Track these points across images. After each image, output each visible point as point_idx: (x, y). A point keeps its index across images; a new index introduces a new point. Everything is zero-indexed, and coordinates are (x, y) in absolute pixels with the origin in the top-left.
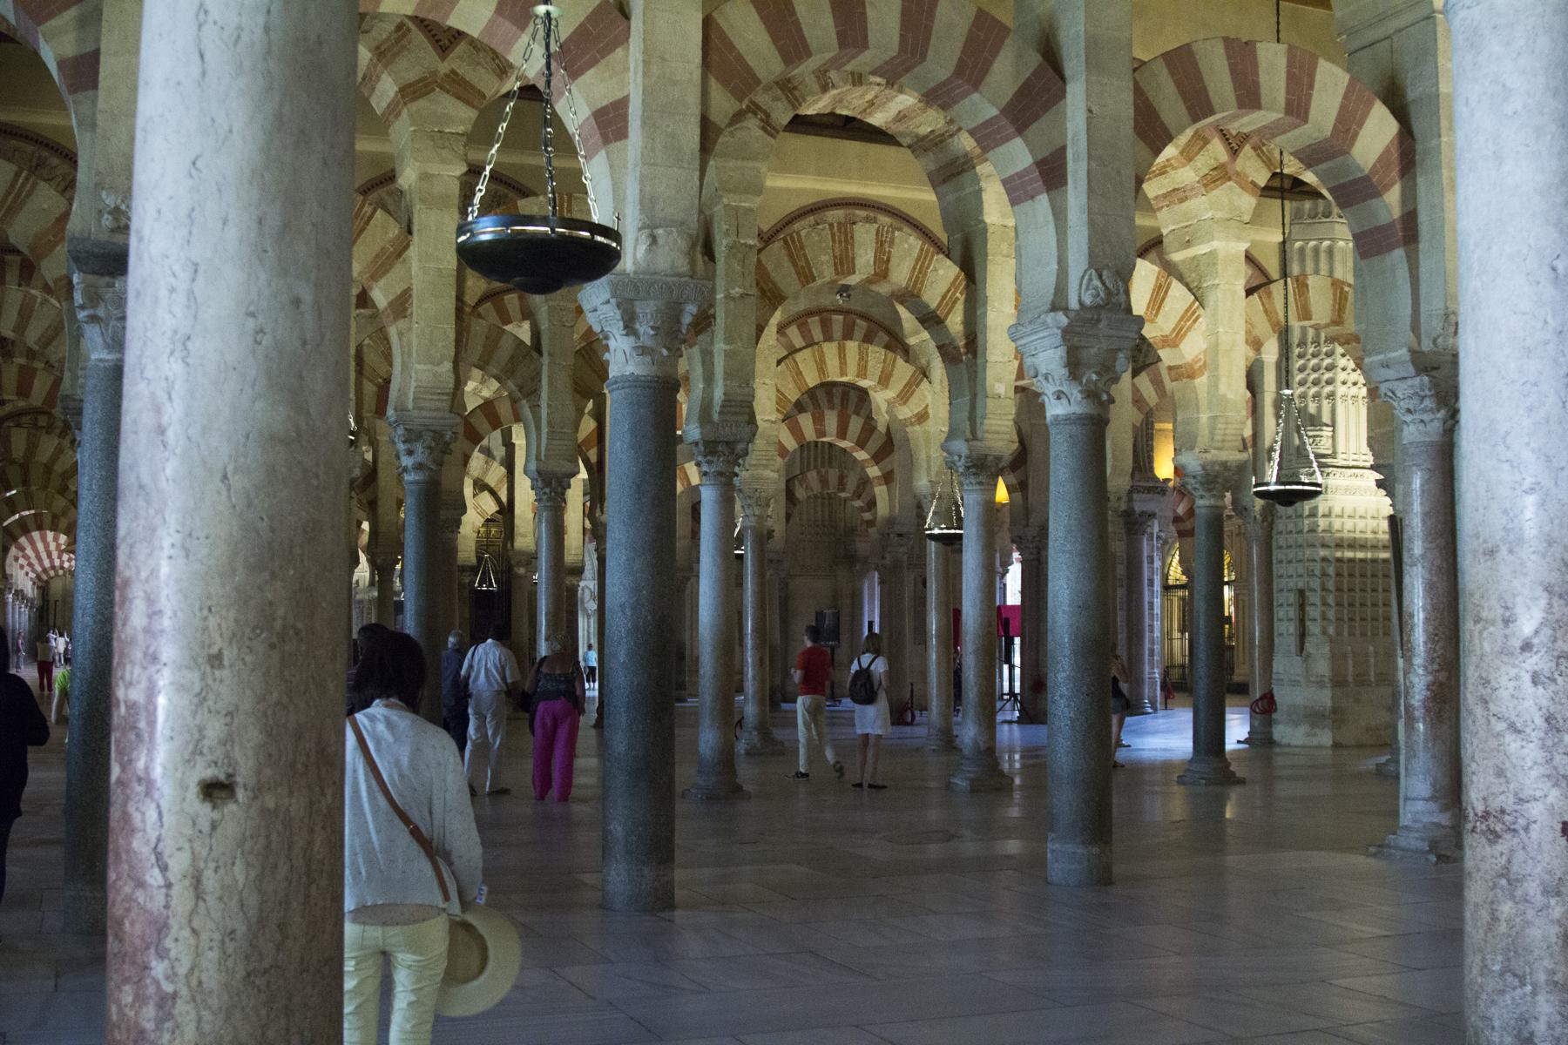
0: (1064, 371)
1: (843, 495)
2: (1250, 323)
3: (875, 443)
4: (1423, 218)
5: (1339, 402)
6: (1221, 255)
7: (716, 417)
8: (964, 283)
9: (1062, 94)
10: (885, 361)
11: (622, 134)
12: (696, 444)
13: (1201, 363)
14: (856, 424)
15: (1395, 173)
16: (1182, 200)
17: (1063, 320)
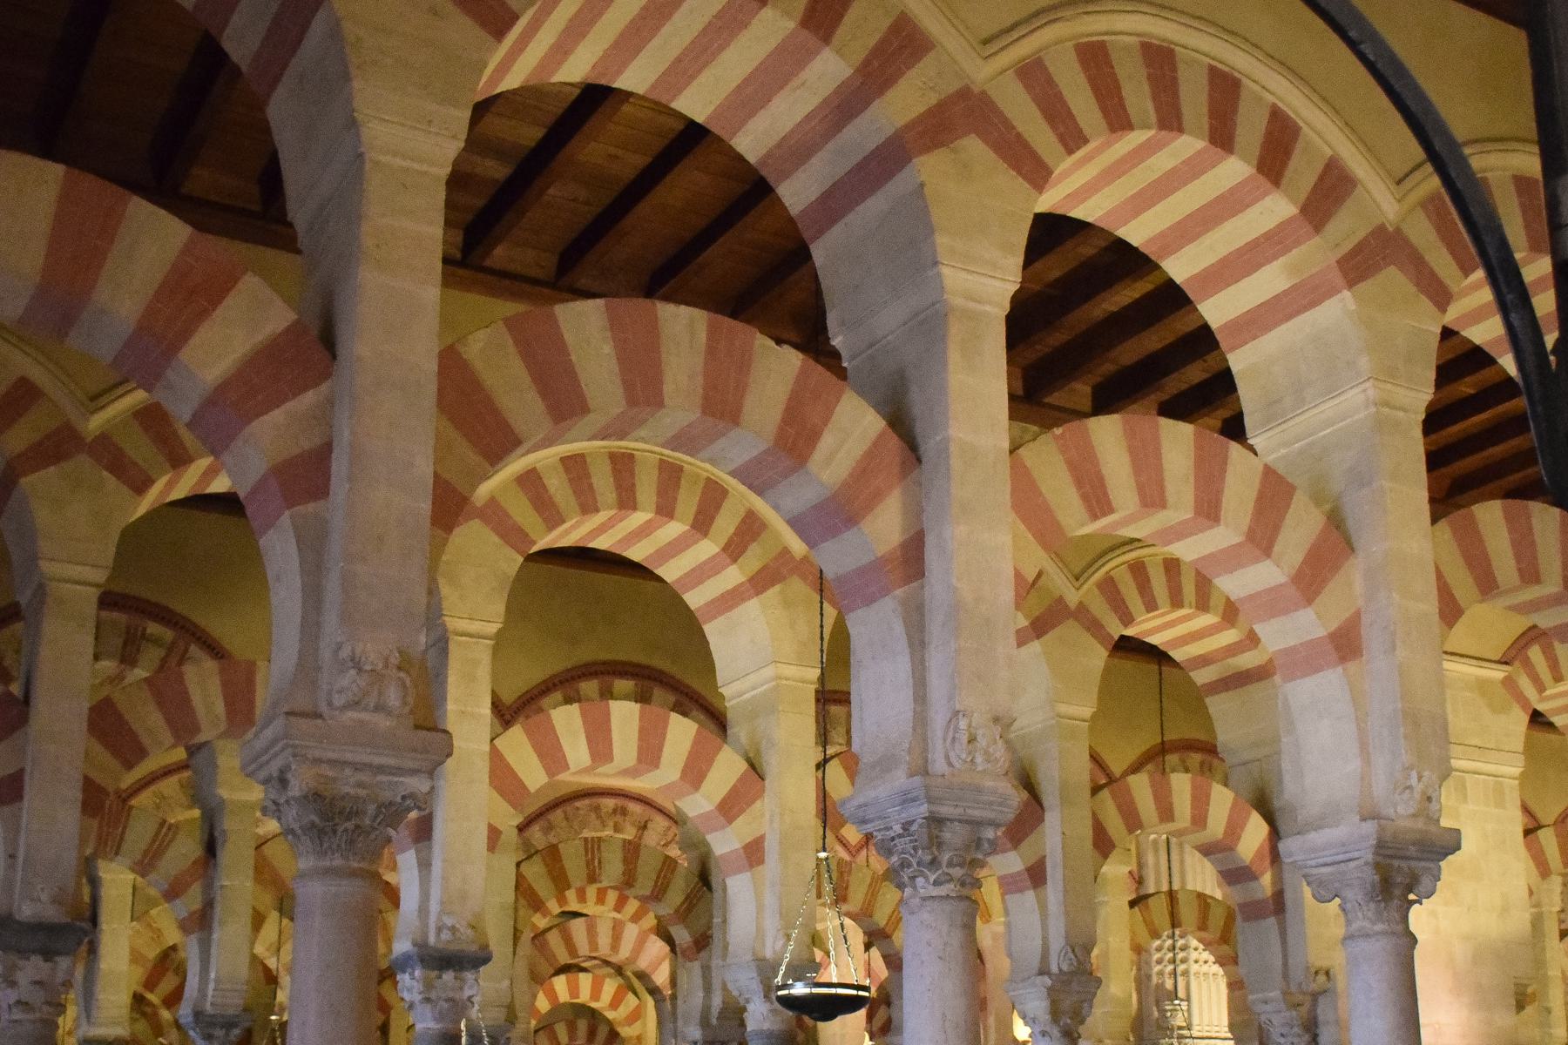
0: (1048, 1017)
2: (1133, 934)
4: (1288, 896)
5: (1192, 978)
7: (714, 1021)
9: (1041, 820)
11: (761, 861)
15: (1267, 862)
17: (1049, 982)
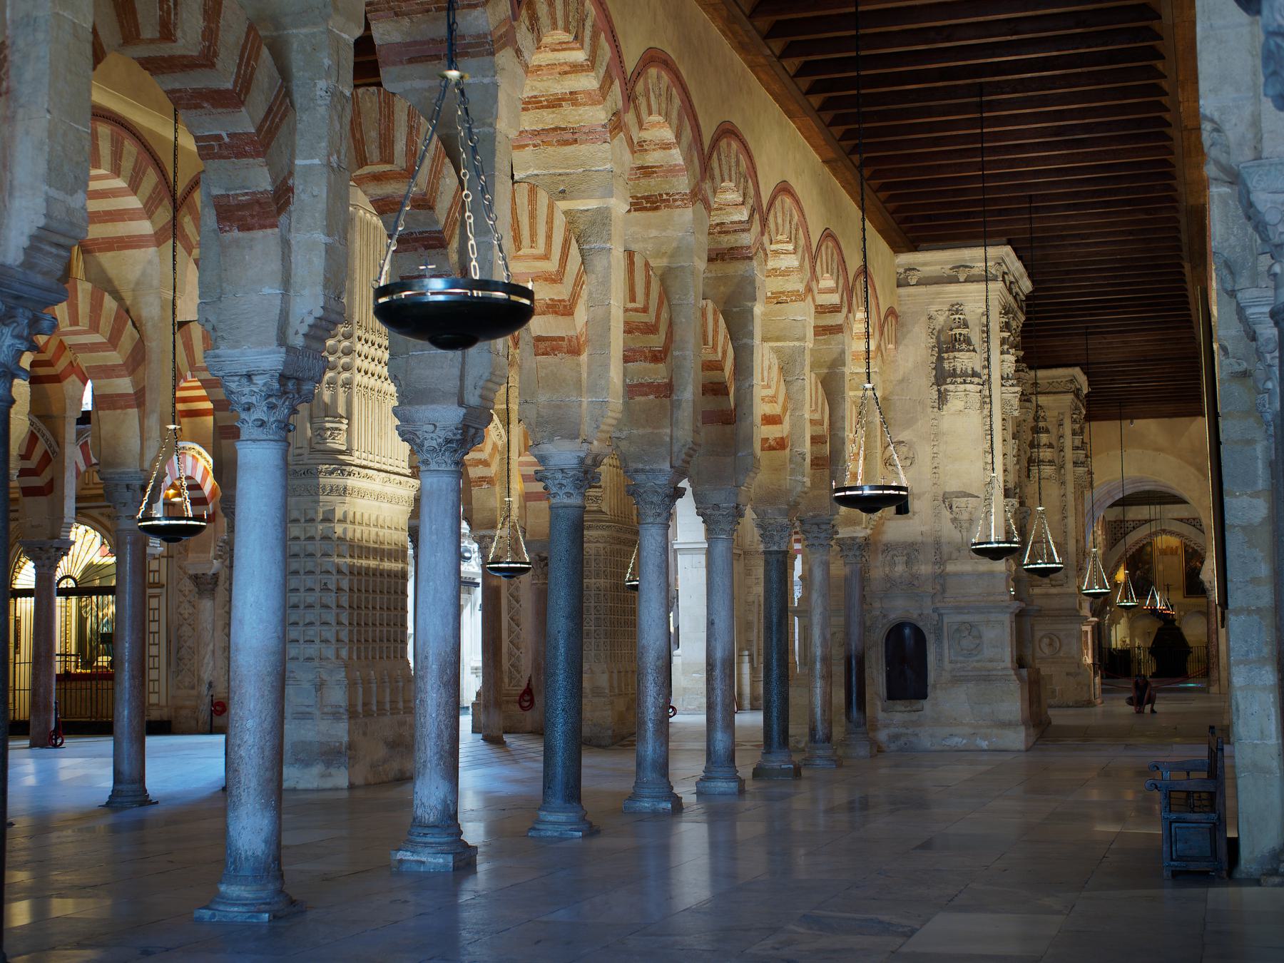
12: (249, 376)
16: (566, 143)
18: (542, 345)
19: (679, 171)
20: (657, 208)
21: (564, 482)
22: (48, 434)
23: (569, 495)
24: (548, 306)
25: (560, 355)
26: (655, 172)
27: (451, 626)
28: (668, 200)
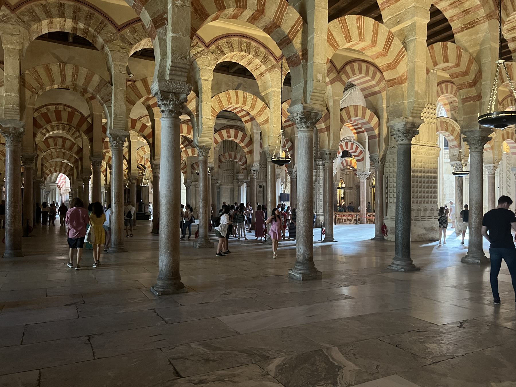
1: (236, 160)
3: (247, 140)
6: (418, 24)
8: (302, 23)
10: (253, 99)
13: (405, 77)
14: (240, 134)
18: (390, 83)
19: (479, 7)
20: (473, 26)
21: (400, 135)
22: (361, 146)
23: (402, 140)
24: (387, 67)
25: (396, 86)
26: (470, 11)
27: (305, 189)
28: (477, 22)
